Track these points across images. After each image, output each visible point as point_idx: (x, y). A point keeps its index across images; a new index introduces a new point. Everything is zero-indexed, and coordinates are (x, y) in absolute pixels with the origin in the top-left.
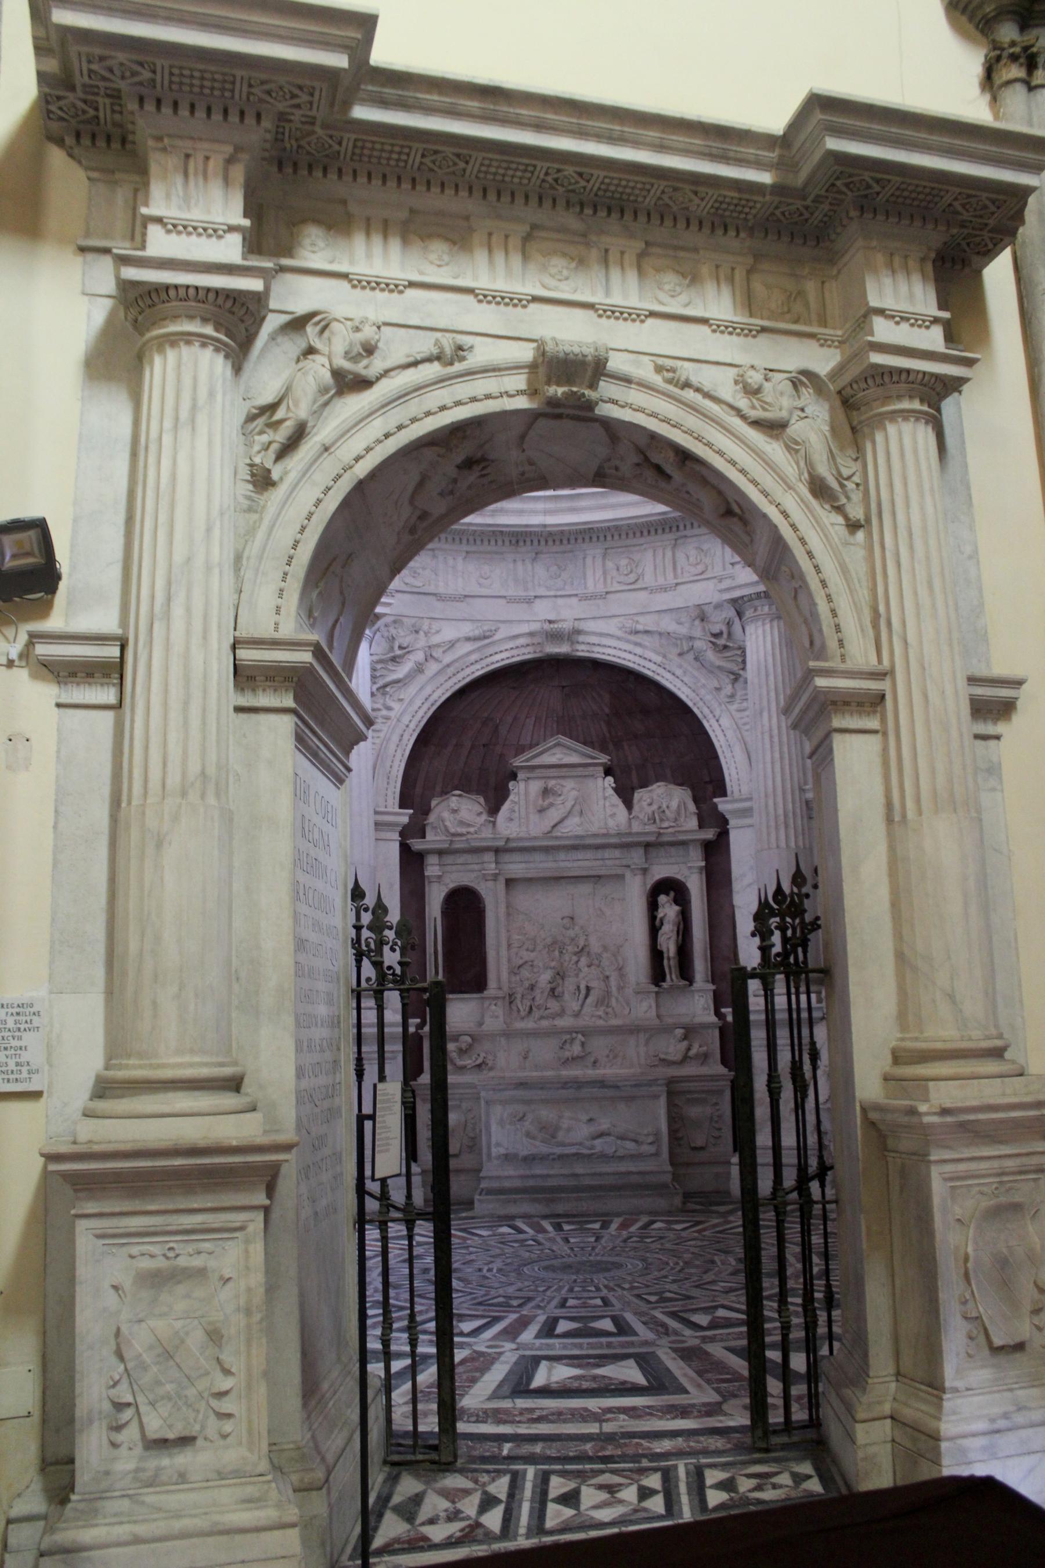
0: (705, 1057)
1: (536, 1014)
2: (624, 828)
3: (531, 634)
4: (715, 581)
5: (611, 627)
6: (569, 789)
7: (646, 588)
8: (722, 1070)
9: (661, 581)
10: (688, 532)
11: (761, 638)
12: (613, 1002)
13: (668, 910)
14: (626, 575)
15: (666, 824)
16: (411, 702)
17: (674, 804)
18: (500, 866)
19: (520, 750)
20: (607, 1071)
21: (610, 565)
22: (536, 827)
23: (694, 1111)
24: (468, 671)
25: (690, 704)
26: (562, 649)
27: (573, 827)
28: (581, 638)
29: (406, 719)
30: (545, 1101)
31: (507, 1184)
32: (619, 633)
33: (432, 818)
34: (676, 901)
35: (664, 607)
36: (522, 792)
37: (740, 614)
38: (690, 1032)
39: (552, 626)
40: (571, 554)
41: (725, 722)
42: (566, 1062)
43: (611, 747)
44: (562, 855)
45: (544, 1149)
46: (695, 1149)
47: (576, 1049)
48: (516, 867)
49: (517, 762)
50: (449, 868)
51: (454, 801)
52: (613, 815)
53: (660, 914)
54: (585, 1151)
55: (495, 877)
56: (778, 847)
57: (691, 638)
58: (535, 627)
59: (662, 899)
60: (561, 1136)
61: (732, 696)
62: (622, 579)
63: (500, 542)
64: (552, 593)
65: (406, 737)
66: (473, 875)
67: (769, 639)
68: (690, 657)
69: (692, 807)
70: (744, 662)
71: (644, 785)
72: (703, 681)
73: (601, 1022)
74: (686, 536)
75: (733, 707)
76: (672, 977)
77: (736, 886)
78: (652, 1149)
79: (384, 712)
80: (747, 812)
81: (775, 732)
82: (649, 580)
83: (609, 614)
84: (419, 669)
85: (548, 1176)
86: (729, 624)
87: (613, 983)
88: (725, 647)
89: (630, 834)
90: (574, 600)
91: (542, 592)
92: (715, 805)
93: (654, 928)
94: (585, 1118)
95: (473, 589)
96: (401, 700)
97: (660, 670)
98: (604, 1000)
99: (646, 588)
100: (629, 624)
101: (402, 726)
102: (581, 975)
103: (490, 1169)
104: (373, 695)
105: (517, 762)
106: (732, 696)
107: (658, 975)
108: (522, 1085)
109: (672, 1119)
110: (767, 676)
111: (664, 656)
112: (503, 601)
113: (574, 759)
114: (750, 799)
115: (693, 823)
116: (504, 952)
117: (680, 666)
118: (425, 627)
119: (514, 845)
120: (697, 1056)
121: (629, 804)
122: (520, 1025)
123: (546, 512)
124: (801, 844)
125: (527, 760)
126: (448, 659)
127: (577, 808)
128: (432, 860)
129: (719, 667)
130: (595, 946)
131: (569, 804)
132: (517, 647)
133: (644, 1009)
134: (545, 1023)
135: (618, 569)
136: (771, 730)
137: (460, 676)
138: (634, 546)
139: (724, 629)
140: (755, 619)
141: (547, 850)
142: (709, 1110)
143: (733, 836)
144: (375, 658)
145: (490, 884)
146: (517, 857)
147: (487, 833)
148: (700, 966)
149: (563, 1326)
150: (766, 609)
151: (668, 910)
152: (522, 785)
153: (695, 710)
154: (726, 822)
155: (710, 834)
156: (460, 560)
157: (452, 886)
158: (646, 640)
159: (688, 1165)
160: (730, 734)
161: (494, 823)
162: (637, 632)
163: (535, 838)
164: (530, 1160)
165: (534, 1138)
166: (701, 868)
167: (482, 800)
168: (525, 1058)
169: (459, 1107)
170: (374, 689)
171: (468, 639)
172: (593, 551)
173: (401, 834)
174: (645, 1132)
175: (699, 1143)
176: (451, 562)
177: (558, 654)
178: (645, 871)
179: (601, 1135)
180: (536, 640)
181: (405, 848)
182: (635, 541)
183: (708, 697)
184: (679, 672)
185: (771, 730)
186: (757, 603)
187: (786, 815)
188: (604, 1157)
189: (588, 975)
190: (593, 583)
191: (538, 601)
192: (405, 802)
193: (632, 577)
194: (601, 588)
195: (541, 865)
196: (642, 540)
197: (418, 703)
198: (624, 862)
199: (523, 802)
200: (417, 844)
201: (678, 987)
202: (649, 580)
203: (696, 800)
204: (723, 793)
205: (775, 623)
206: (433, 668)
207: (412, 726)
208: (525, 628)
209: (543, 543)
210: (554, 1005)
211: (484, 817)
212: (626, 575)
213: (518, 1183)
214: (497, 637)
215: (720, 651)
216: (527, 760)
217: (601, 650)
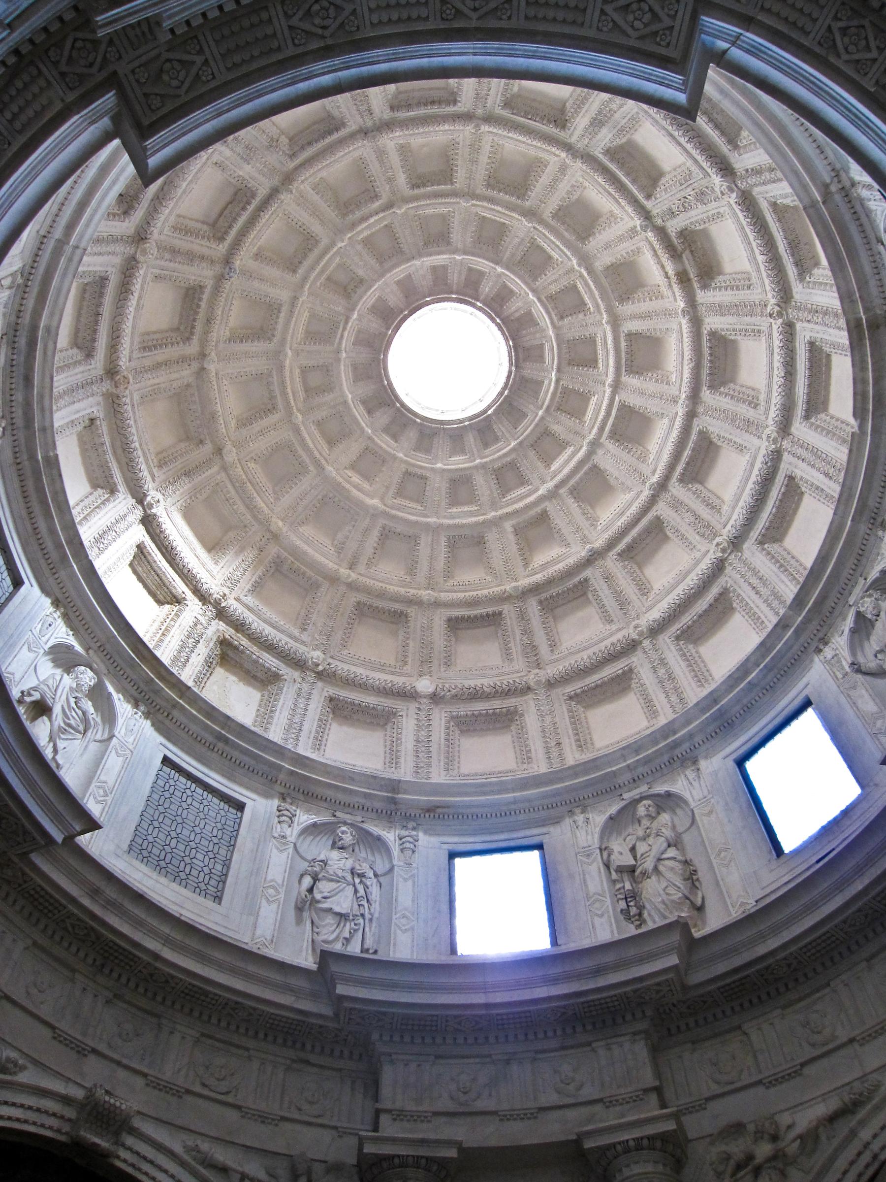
3: (66, 1100)
4: (334, 1132)
7: (238, 1108)
10: (313, 1058)
14: (218, 1080)
26: (103, 1143)
28: (130, 1141)
32: (186, 1157)
35: (257, 1145)
39: (107, 1098)
58: (79, 1094)
62: (211, 1082)
63: (82, 954)
64: (115, 1056)
74: (307, 1062)
83: (179, 1122)
90: (140, 1082)
91: (102, 1047)
95: (18, 995)
99: (238, 1108)
100: (205, 1146)
112: (47, 1033)
123: (167, 941)
132: (38, 1110)
135: (207, 1067)
138: (238, 1047)
180: (70, 1113)
191: (92, 1058)
193: (223, 1086)
196: (251, 1044)
208: (59, 1087)
209: (132, 985)
212: (218, 1080)
214: (23, 1078)
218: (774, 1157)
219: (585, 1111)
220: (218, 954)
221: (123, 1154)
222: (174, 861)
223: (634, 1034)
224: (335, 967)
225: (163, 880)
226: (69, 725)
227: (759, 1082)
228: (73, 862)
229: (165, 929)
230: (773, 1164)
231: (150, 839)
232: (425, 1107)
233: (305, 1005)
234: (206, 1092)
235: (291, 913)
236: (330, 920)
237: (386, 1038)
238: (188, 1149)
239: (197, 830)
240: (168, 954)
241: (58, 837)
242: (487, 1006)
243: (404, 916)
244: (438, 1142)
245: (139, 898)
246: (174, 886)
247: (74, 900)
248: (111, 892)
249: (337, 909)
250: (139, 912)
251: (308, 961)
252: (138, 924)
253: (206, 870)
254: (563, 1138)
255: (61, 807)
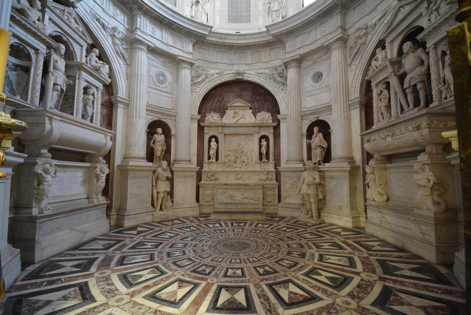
0: (271, 179)
1: (231, 167)
2: (254, 122)
3: (233, 73)
5: (253, 72)
6: (241, 112)
8: (276, 183)
9: (266, 60)
10: (274, 47)
11: (292, 73)
12: (249, 165)
13: (264, 143)
15: (264, 122)
16: (202, 88)
17: (267, 117)
18: (224, 131)
19: (229, 102)
20: (247, 182)
21: (253, 56)
22: (232, 121)
23: (269, 193)
24: (216, 82)
25: (272, 92)
26: (240, 77)
27: (241, 121)
28: (245, 75)
29: (200, 92)
30: (231, 189)
31: (220, 210)
32: (255, 74)
33: (207, 118)
34: (266, 141)
36: (229, 113)
37: (286, 67)
38: (268, 173)
40: (243, 54)
41: (280, 96)
42: (237, 179)
43: (252, 103)
44: (238, 129)
45: (231, 201)
46: (268, 202)
47: (240, 176)
48: (227, 131)
49: (228, 105)
50: (209, 131)
51: (212, 114)
52: (251, 119)
53: (262, 144)
54: (241, 202)
55: (222, 133)
56: (293, 126)
57: (273, 74)
58: (234, 72)
59: (263, 140)
60: (235, 198)
61: (283, 89)
62: (256, 60)
65: (200, 97)
66: (216, 132)
67: (294, 72)
68: (273, 79)
69: (271, 118)
70: (286, 80)
71: (259, 112)
72: (276, 85)
73: (246, 170)
74: (273, 48)
75: (282, 92)
76: (264, 160)
77: (281, 137)
78: (258, 202)
79: (194, 90)
80: (285, 118)
81: (294, 96)
82: (263, 60)
84: (204, 80)
85: (231, 208)
86: (283, 70)
87: (250, 161)
88: (282, 76)
89: (255, 123)
90: (244, 65)
92: (277, 117)
93: (260, 147)
94: (241, 193)
95: (219, 61)
96: (199, 87)
97: (264, 83)
98: (247, 164)
100: (257, 71)
101: (199, 94)
102: (242, 158)
103: (217, 206)
104: (191, 85)
105: (228, 105)
106: (283, 89)
107: (261, 159)
108: (226, 184)
109: (263, 194)
110: (293, 82)
111: (266, 79)
112: (226, 65)
113: (242, 105)
114: (286, 115)
115: (271, 121)
116: (223, 152)
117: (270, 82)
118: (206, 69)
119: (226, 125)
120: (270, 179)
121: (255, 117)
122: (226, 170)
123: (237, 40)
124: (299, 126)
125: (230, 105)
126: (211, 79)
127: (243, 117)
128: (206, 128)
129: (280, 82)
130: (245, 151)
131: (240, 116)
133: (257, 168)
134: (233, 169)
136: (293, 96)
137: (214, 83)
139: (282, 71)
140: (290, 67)
141: (234, 127)
142: (272, 192)
143: (281, 124)
144: (192, 76)
145: (220, 135)
146: (227, 128)
147: (220, 122)
148: (271, 157)
149: (234, 255)
150: (294, 64)
151: (264, 143)
152: (229, 111)
153: (273, 93)
154: (279, 121)
155: (275, 124)
156: (215, 53)
157: (211, 135)
158: (262, 76)
159: (267, 206)
160: (282, 99)
161: (222, 120)
162: (259, 73)
163: (232, 124)
164: (226, 204)
165: (228, 198)
166: (273, 133)
167: (219, 114)
168: (227, 178)
169: (210, 189)
170: (192, 83)
171: (217, 74)
172: (249, 53)
173: (199, 121)
174: (257, 197)
175: (270, 200)
176: (213, 53)
177: (239, 79)
178: (258, 133)
179: (245, 198)
181: (199, 125)
182: (260, 50)
183: (276, 90)
184: (269, 84)
185: (293, 96)
186: (291, 63)
187: (296, 118)
188: (245, 204)
189: (244, 158)
190: (249, 61)
192: (199, 113)
193: (259, 60)
194: (251, 62)
195: (234, 131)
196: (262, 49)
197: (203, 88)
198: (253, 131)
199: (229, 115)
200: (202, 124)
201: (266, 162)
202: (263, 60)
203: (272, 116)
204: (279, 113)
205: (296, 68)
206: (208, 80)
207: (202, 94)
208: (231, 72)
210: (235, 165)
211: (219, 118)
213: (223, 210)
214: (225, 73)
215: (280, 78)
216: (230, 105)
217: (250, 78)
218: (365, 34)
219: (325, 37)
220: (247, 37)
221: (245, 77)
222: (239, 18)
223: (337, 14)
224: (269, 29)
225: (237, 24)
226: (204, 2)
227: (366, 15)
228: (214, 35)
229: (236, 37)
230: (365, 35)
231: (232, 16)
232: (294, 49)
233: (268, 38)
234: (256, 62)
235: (266, 15)
236: (274, 13)
237: (285, 38)
238: (255, 73)
239: (242, 7)
240: (239, 42)
241: (207, 33)
242: (302, 22)
243: (291, 3)
244: (295, 56)
245: (228, 34)
246: (240, 24)
247: (218, 42)
248: (223, 36)
249: (275, 9)
250: (230, 37)
251: (265, 29)
252: (231, 39)
253: (246, 16)
254: (320, 45)
255: (204, 28)
